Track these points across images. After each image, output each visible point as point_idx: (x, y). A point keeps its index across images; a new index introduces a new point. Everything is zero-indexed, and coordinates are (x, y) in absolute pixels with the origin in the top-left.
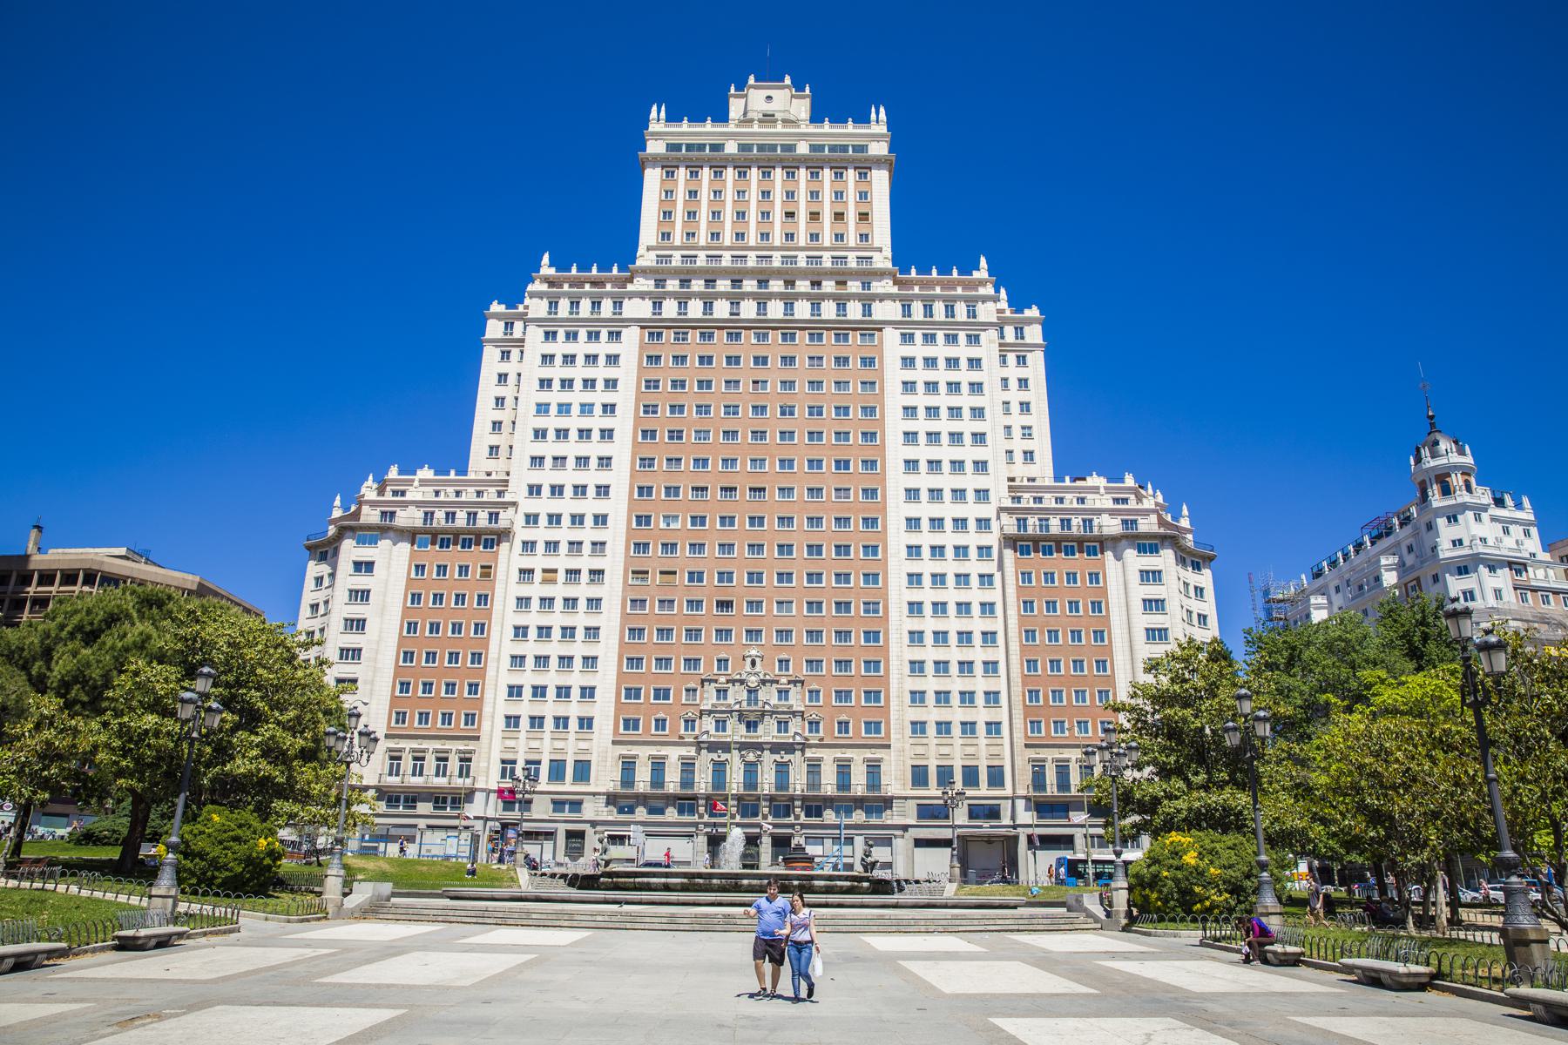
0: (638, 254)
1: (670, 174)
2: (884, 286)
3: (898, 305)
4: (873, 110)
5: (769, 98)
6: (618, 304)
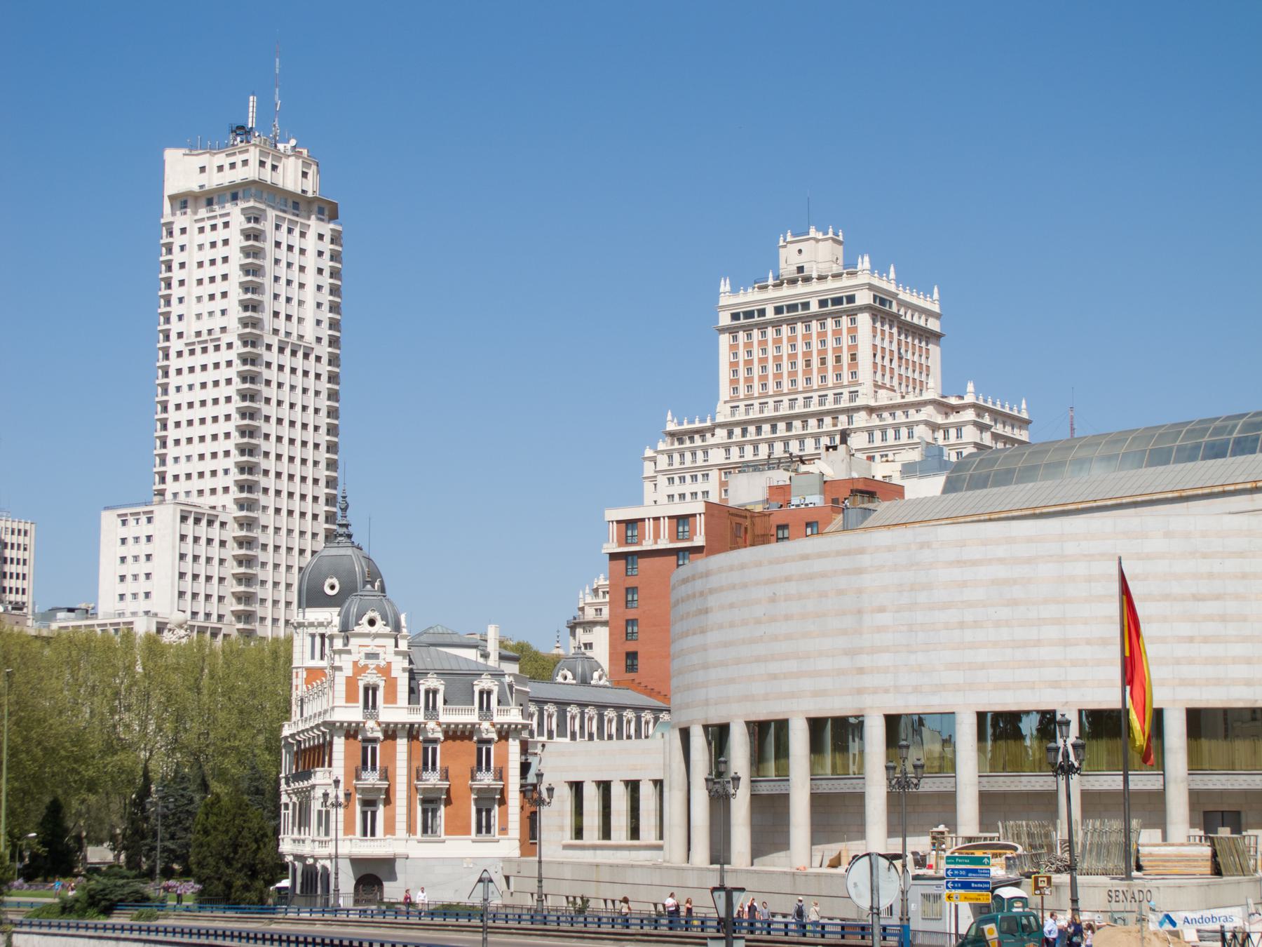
0: (718, 410)
1: (735, 338)
2: (861, 419)
3: (866, 435)
4: (860, 259)
5: (800, 251)
6: (706, 453)
